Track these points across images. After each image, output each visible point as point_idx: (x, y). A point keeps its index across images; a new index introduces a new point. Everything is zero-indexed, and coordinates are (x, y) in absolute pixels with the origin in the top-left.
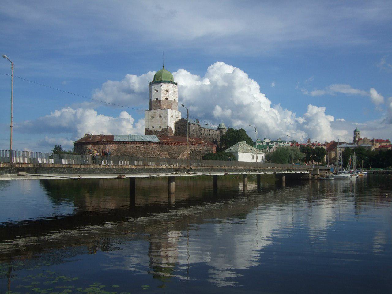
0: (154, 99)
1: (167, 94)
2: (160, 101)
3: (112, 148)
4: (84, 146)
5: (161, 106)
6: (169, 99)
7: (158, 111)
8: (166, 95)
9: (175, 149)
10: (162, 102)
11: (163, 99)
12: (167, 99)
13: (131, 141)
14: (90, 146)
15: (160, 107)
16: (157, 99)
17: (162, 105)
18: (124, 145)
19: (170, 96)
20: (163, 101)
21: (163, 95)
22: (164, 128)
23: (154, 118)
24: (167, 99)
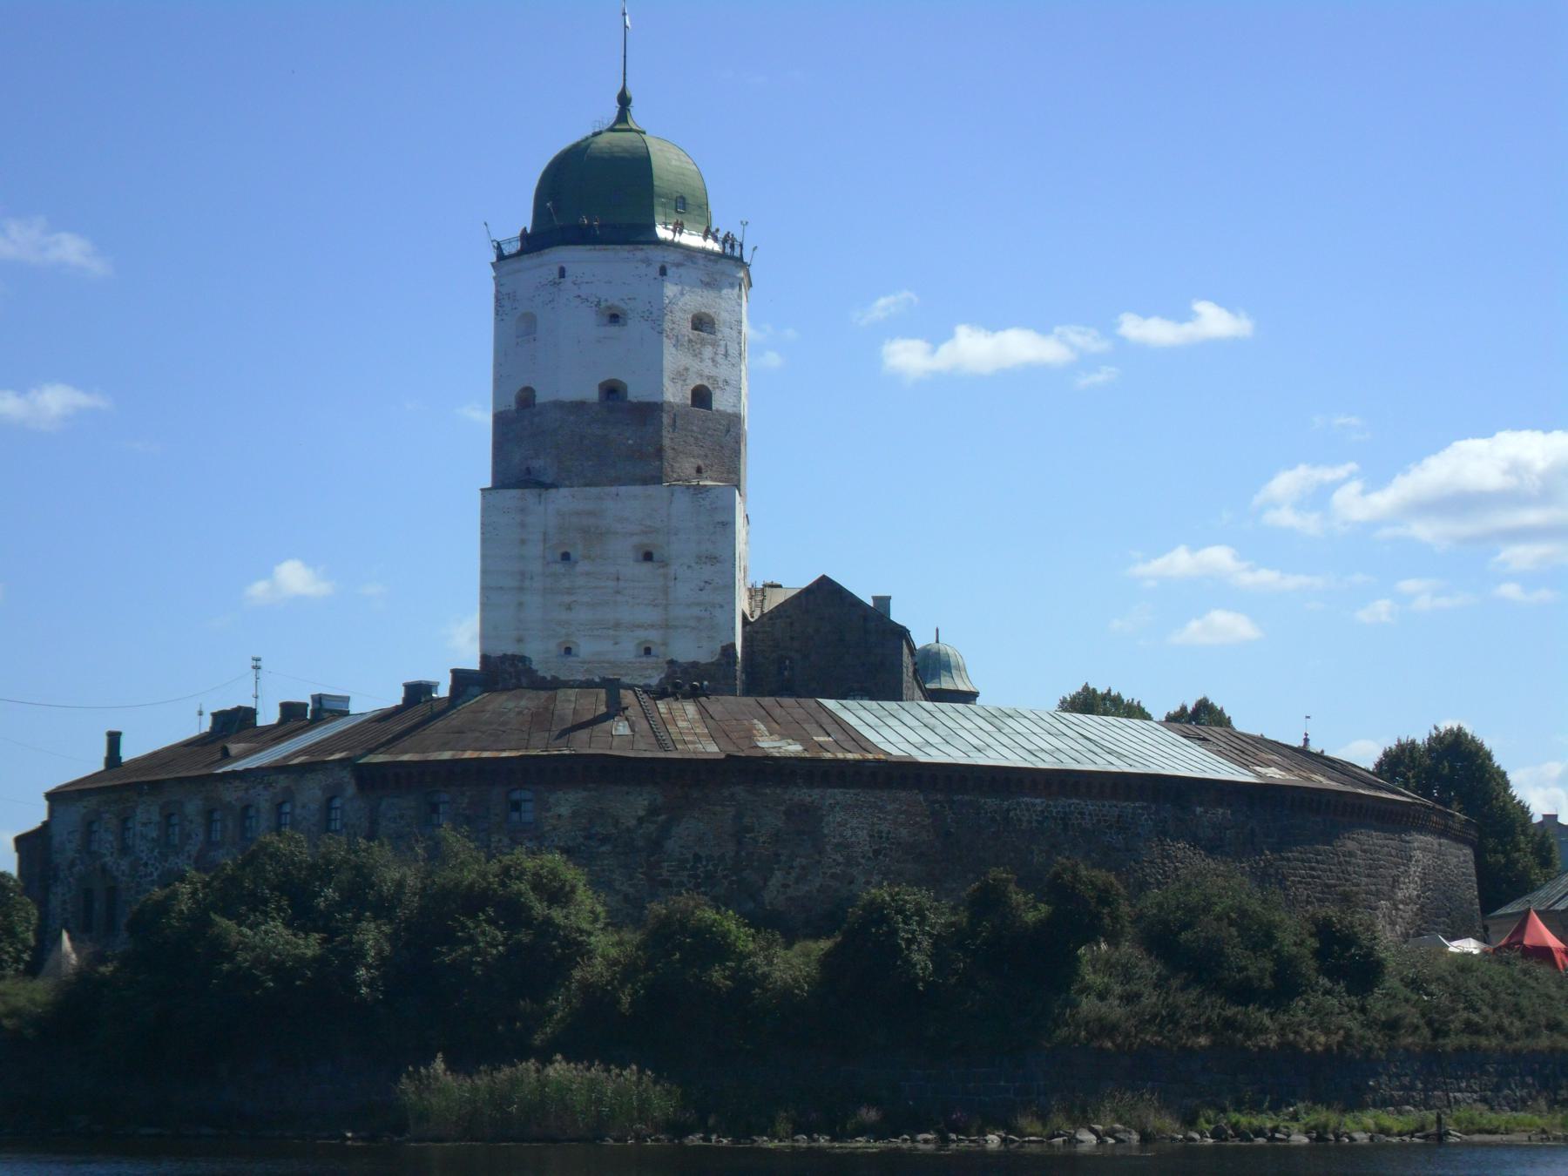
0: (575, 383)
1: (708, 352)
2: (650, 412)
3: (885, 827)
4: (566, 803)
5: (659, 452)
6: (720, 402)
7: (628, 507)
8: (694, 365)
9: (1351, 854)
10: (666, 420)
11: (675, 394)
12: (701, 397)
13: (1048, 763)
14: (632, 806)
15: (646, 465)
16: (612, 391)
17: (669, 453)
18: (990, 803)
19: (723, 371)
20: (677, 415)
21: (672, 358)
22: (695, 664)
23: (582, 567)
24: (701, 397)
